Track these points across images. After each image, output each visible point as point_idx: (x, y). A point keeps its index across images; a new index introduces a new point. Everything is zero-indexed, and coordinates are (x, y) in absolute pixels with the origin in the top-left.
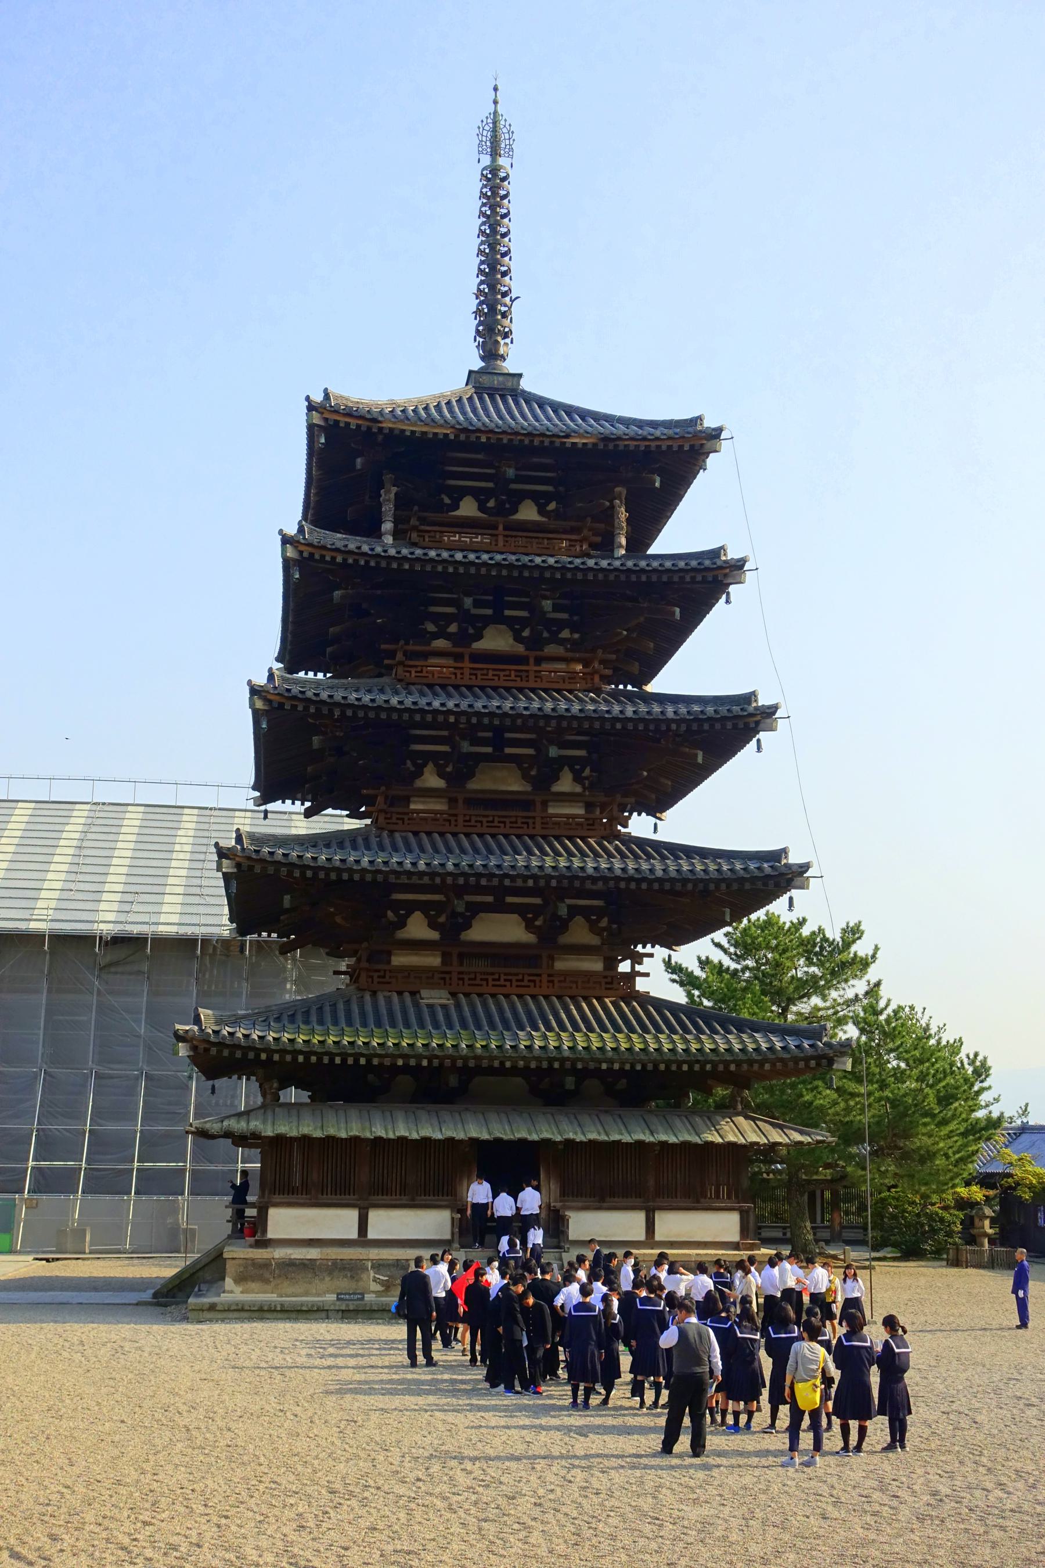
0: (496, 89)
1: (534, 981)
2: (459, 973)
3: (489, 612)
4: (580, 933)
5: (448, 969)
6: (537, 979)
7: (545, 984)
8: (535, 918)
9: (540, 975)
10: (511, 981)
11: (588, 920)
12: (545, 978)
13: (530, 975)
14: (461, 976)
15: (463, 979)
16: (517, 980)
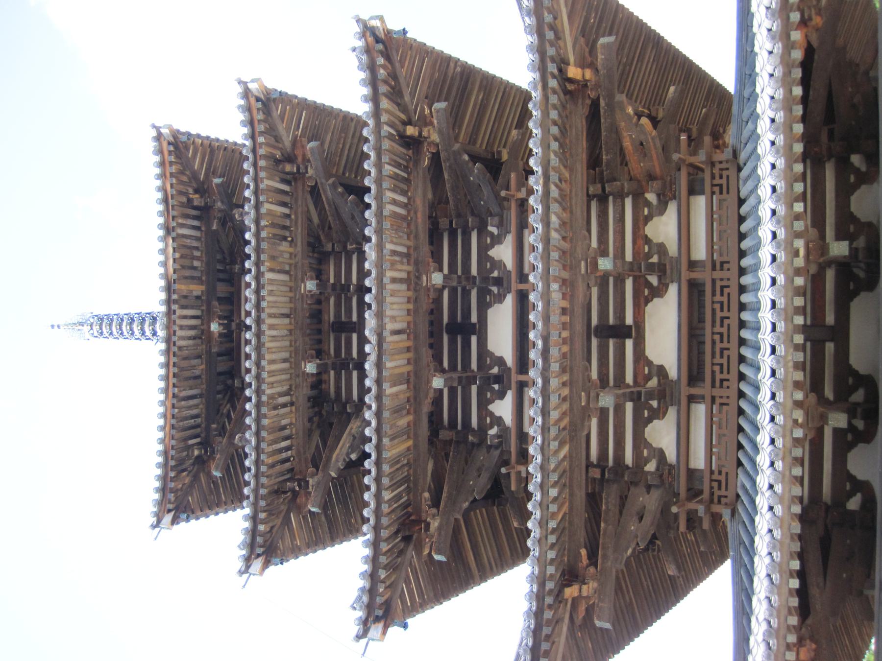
0: (53, 326)
1: (722, 287)
2: (713, 386)
3: (355, 336)
4: (664, 229)
5: (708, 399)
6: (719, 284)
7: (724, 274)
8: (649, 285)
9: (714, 281)
10: (722, 319)
11: (648, 219)
12: (717, 274)
13: (714, 294)
14: (718, 384)
15: (722, 381)
16: (722, 310)
